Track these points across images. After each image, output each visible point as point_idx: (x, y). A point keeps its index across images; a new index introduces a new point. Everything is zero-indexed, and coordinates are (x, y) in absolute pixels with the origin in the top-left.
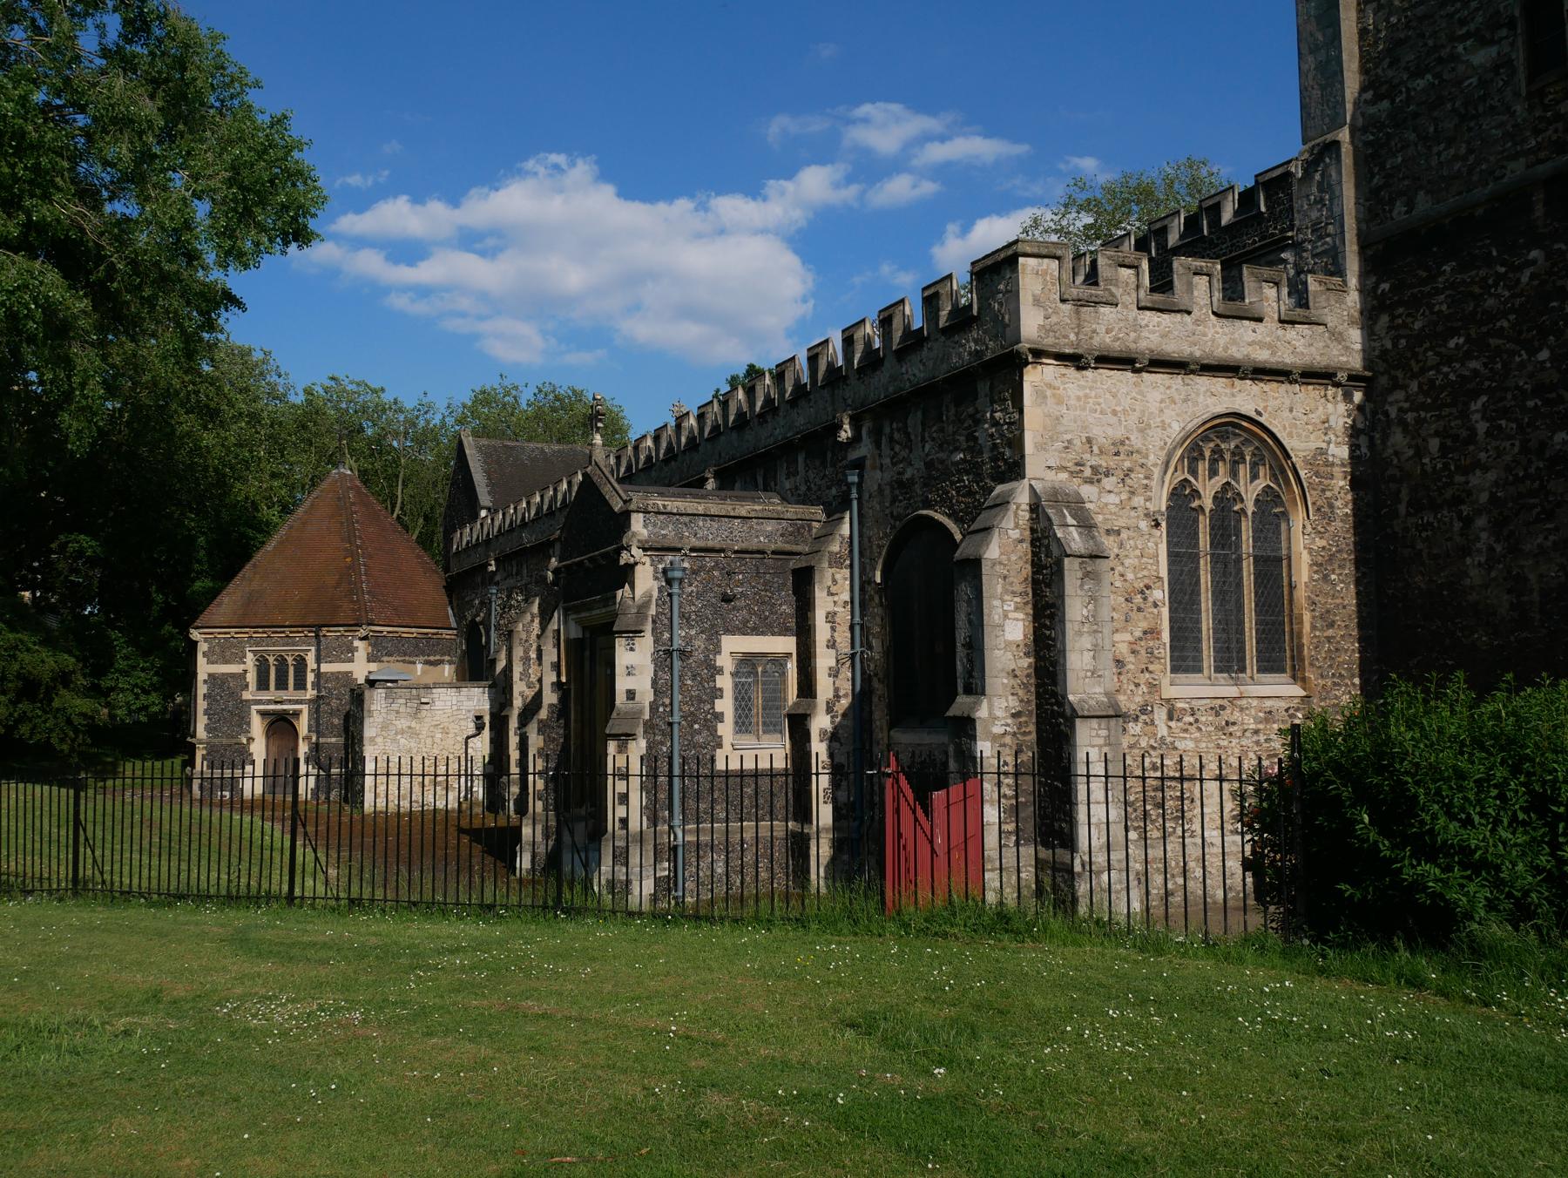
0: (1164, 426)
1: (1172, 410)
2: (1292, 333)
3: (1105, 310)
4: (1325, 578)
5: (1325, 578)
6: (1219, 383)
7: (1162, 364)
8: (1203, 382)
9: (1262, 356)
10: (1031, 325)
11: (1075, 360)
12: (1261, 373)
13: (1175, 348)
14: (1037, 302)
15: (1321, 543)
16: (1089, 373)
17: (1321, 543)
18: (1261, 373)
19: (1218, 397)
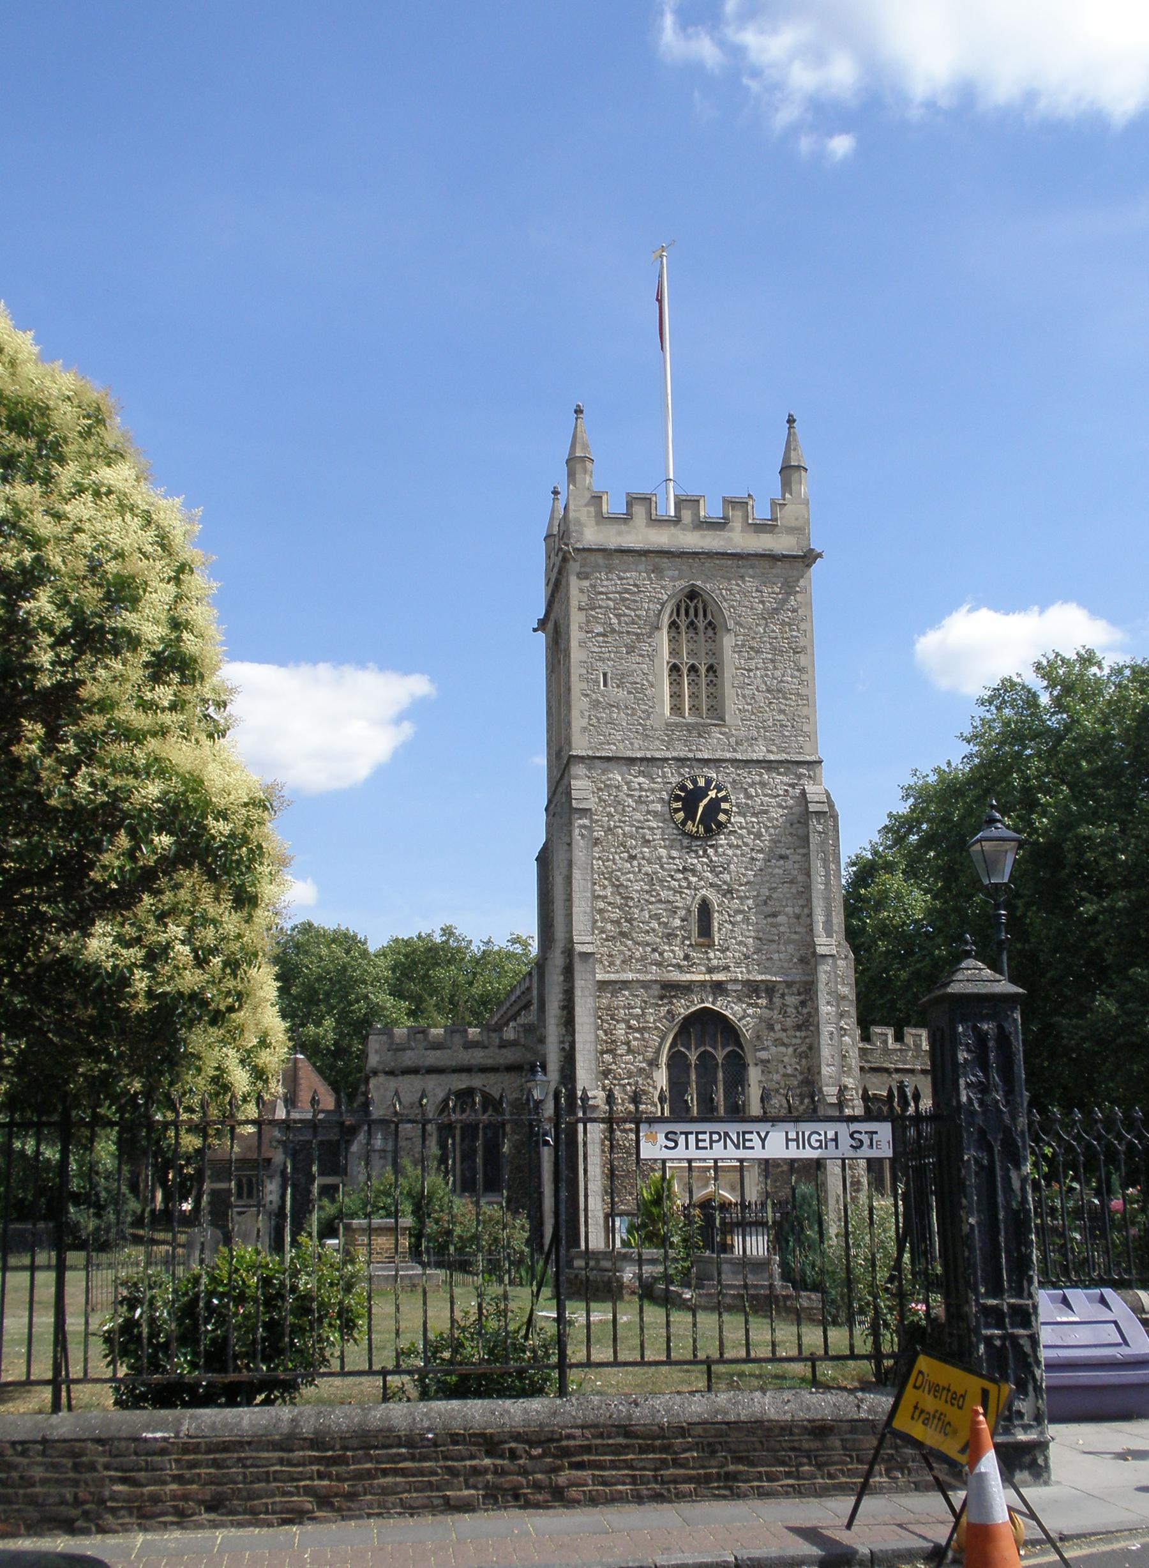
0: (435, 1095)
1: (437, 1089)
2: (504, 1051)
3: (409, 1052)
4: (519, 1152)
5: (519, 1152)
6: (464, 1076)
7: (432, 1070)
8: (455, 1076)
9: (490, 1062)
10: (373, 1060)
11: (391, 1073)
12: (483, 1070)
13: (441, 1063)
14: (376, 1052)
15: (517, 1137)
16: (400, 1078)
17: (517, 1137)
18: (483, 1070)
19: (461, 1082)
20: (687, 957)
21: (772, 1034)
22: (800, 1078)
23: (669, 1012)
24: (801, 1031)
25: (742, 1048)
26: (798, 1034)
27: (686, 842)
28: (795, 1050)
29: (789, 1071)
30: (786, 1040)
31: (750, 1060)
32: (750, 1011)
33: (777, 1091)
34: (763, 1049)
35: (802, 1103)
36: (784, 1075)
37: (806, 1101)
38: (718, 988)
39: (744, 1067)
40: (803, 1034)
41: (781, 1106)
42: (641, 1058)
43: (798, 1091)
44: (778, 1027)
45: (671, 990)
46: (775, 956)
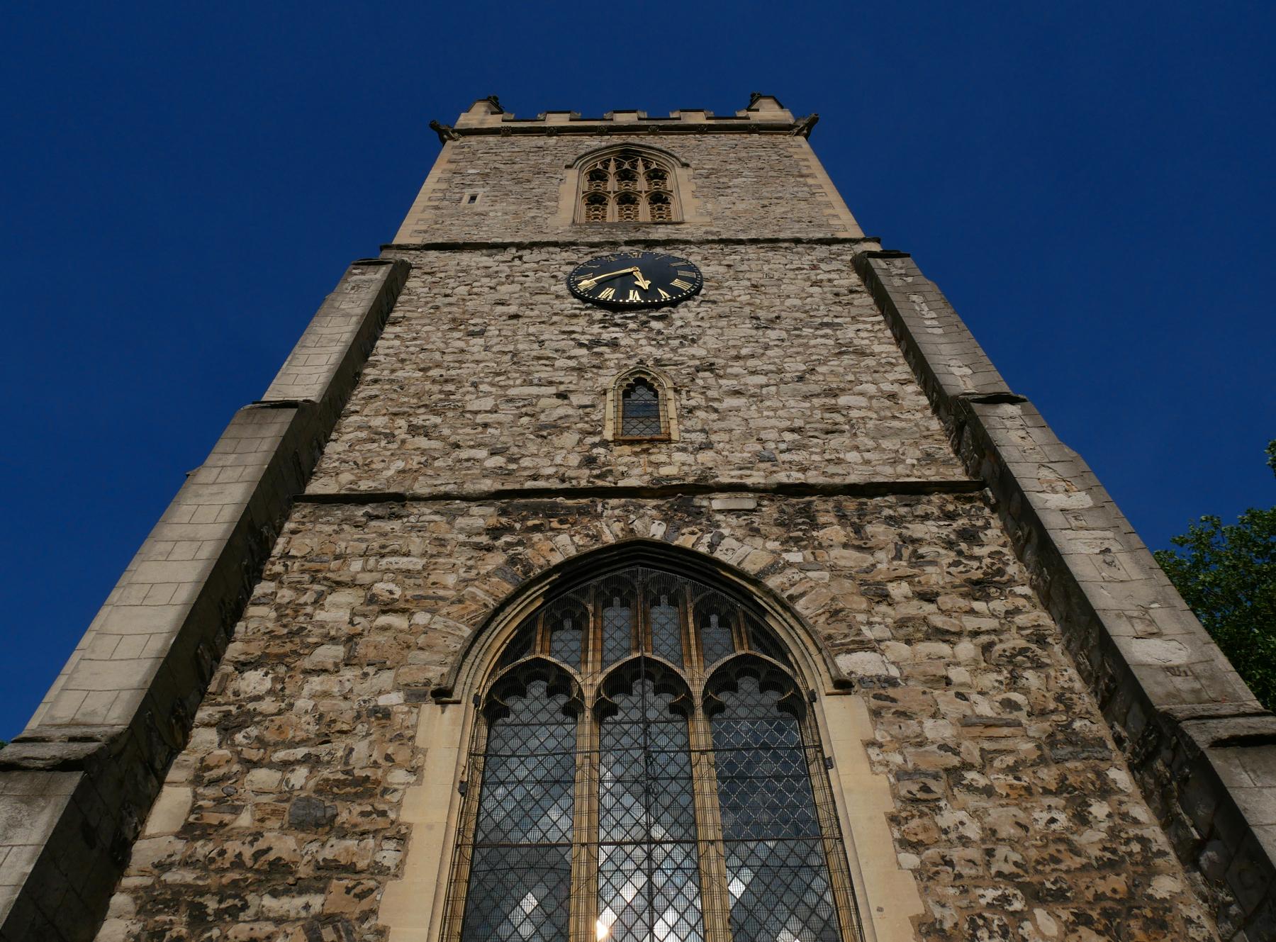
20: (590, 461)
21: (883, 608)
22: (1037, 728)
23: (513, 561)
24: (987, 598)
25: (779, 649)
26: (979, 606)
27: (598, 315)
28: (987, 648)
29: (985, 708)
30: (939, 621)
31: (816, 679)
32: (795, 557)
33: (954, 774)
34: (864, 646)
35: (1082, 819)
36: (965, 722)
37: (1099, 810)
38: (682, 496)
39: (797, 706)
40: (999, 605)
41: (991, 833)
42: (386, 678)
43: (1048, 775)
44: (899, 590)
45: (523, 503)
46: (852, 456)
